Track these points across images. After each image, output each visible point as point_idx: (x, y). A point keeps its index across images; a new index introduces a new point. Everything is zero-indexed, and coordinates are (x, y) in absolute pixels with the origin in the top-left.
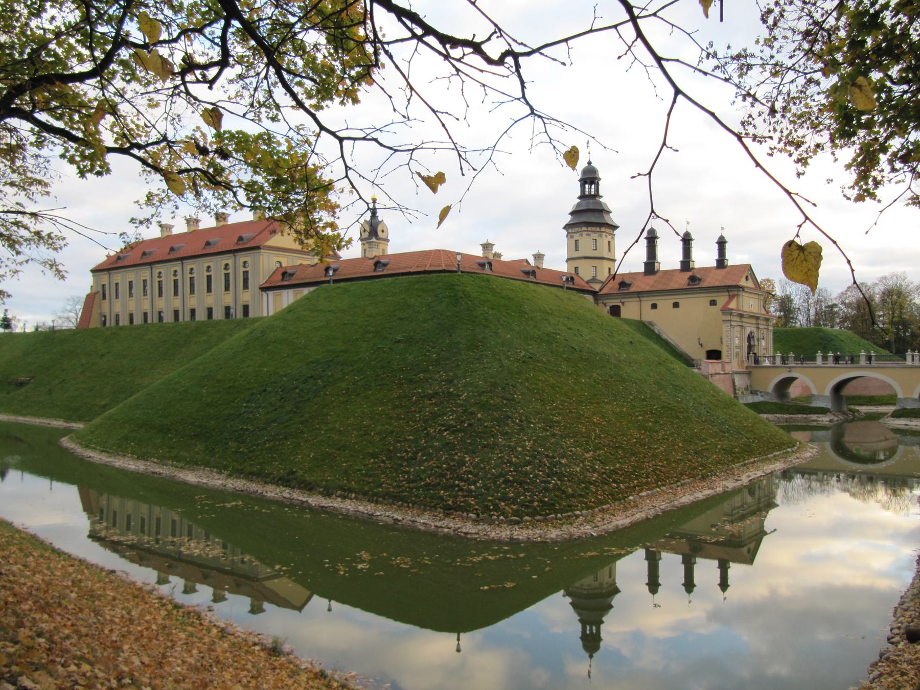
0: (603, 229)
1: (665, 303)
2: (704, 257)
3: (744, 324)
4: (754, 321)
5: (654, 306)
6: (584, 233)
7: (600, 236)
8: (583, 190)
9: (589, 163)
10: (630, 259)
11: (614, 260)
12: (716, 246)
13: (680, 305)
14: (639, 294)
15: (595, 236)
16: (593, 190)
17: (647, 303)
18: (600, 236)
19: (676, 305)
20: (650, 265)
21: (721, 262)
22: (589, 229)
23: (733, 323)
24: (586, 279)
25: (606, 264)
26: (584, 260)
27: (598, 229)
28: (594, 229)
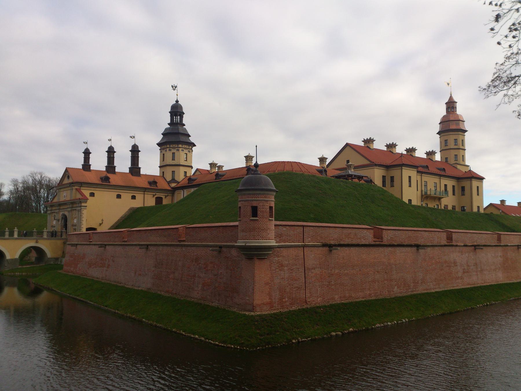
0: (180, 146)
6: (168, 149)
7: (178, 150)
11: (192, 167)
15: (173, 151)
18: (178, 150)
24: (168, 180)
25: (186, 169)
28: (174, 145)
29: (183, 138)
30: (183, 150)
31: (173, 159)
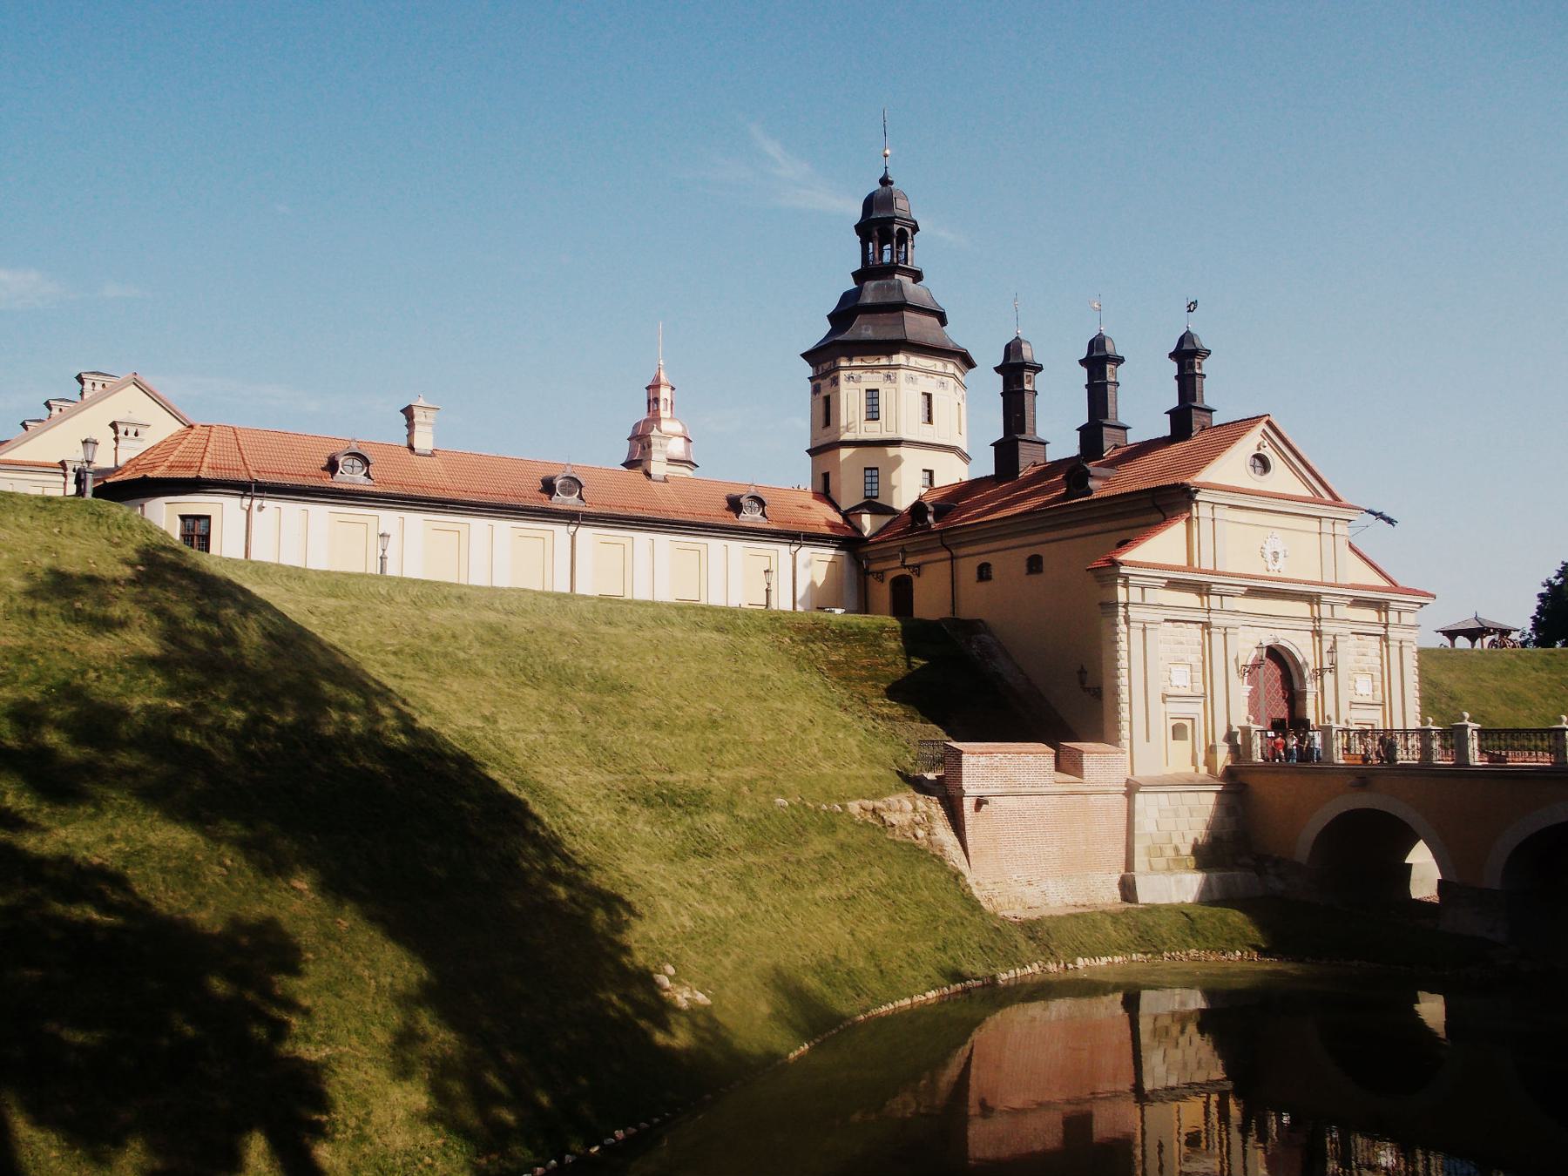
0: (900, 359)
1: (1008, 561)
2: (1143, 408)
3: (1216, 619)
4: (1303, 609)
5: (984, 573)
9: (885, 181)
12: (1173, 367)
13: (1046, 565)
20: (1006, 452)
24: (844, 508)
27: (884, 361)
29: (915, 326)
31: (873, 415)
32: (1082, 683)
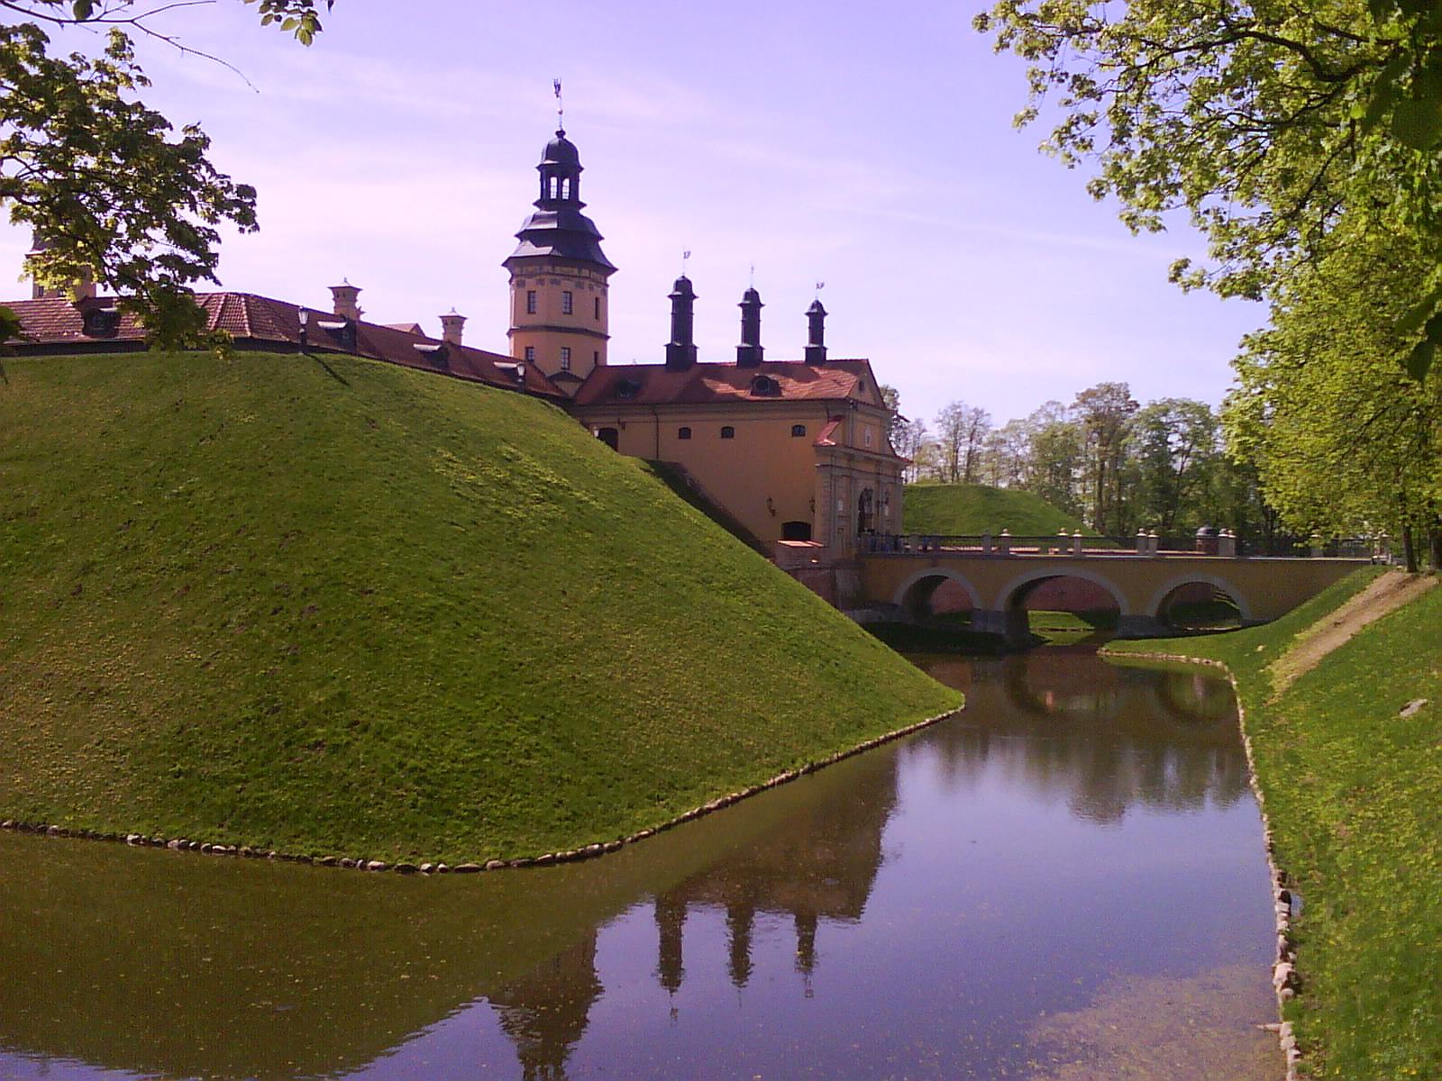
0: (585, 272)
4: (871, 468)
5: (685, 433)
6: (547, 278)
8: (545, 190)
9: (561, 134)
10: (636, 337)
14: (656, 407)
15: (569, 285)
16: (566, 190)
17: (670, 427)
18: (580, 286)
19: (727, 433)
21: (816, 353)
22: (558, 270)
23: (837, 472)
26: (544, 335)
27: (576, 271)
28: (566, 270)
30: (591, 288)
32: (770, 507)
